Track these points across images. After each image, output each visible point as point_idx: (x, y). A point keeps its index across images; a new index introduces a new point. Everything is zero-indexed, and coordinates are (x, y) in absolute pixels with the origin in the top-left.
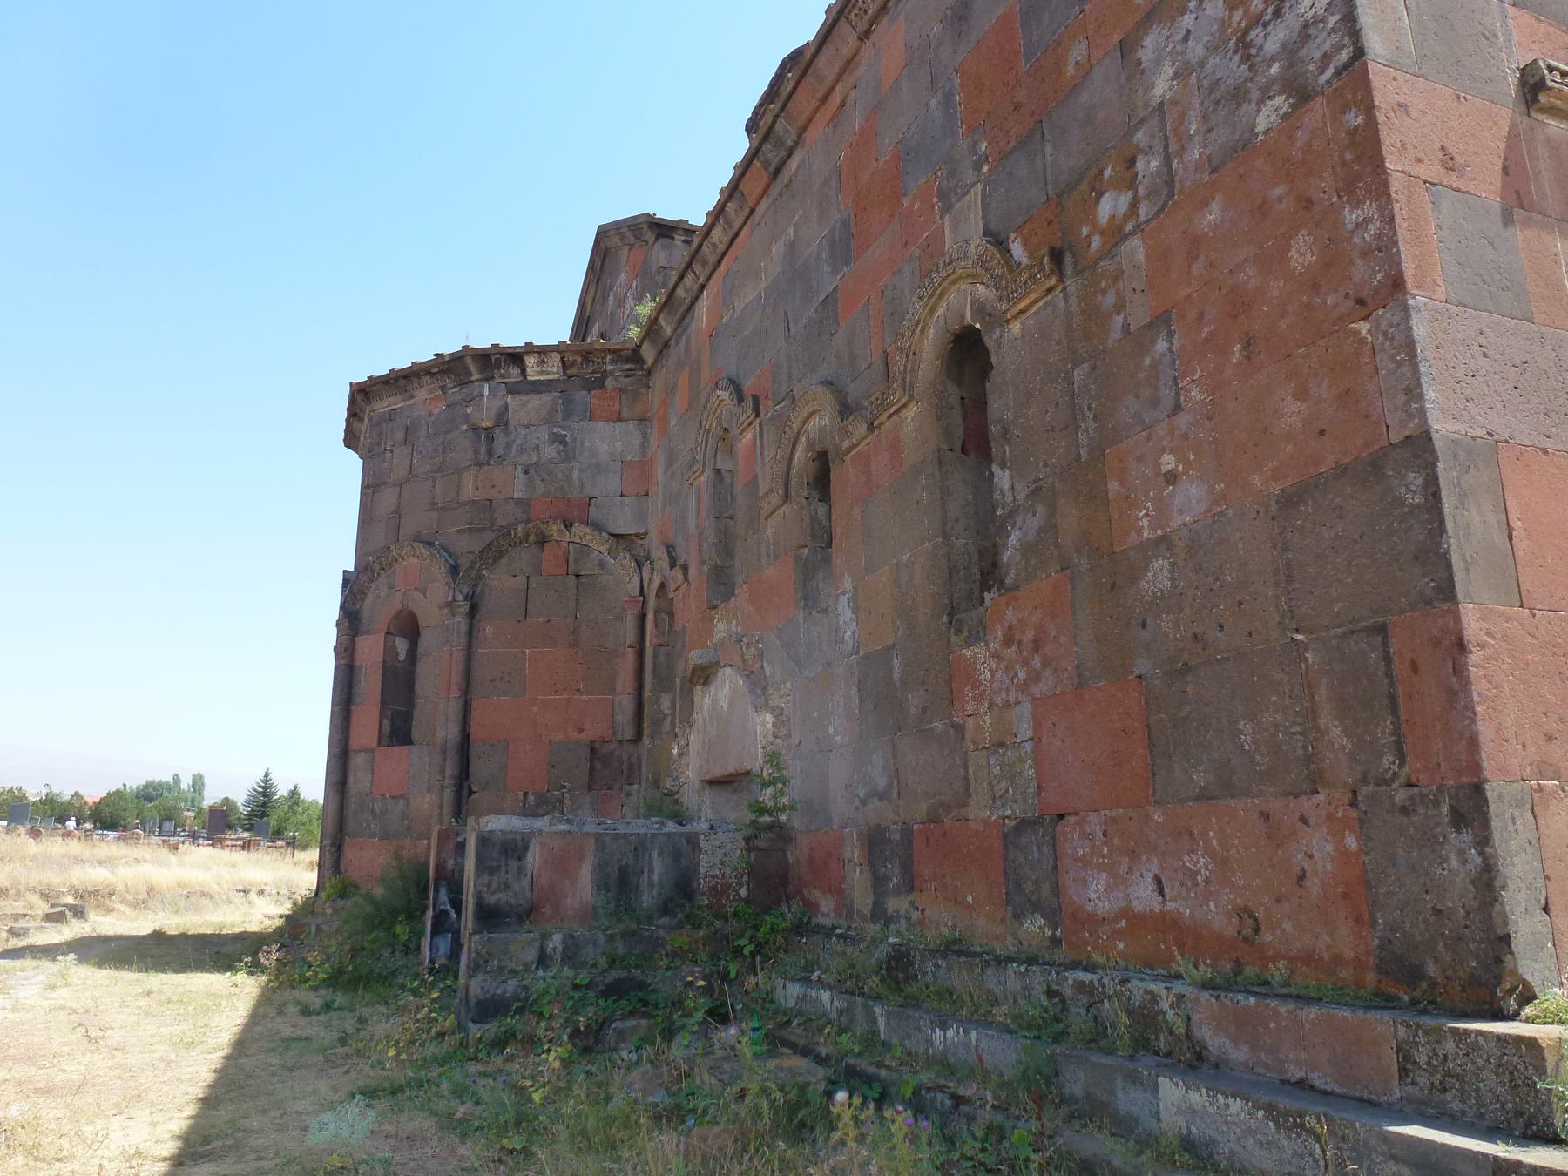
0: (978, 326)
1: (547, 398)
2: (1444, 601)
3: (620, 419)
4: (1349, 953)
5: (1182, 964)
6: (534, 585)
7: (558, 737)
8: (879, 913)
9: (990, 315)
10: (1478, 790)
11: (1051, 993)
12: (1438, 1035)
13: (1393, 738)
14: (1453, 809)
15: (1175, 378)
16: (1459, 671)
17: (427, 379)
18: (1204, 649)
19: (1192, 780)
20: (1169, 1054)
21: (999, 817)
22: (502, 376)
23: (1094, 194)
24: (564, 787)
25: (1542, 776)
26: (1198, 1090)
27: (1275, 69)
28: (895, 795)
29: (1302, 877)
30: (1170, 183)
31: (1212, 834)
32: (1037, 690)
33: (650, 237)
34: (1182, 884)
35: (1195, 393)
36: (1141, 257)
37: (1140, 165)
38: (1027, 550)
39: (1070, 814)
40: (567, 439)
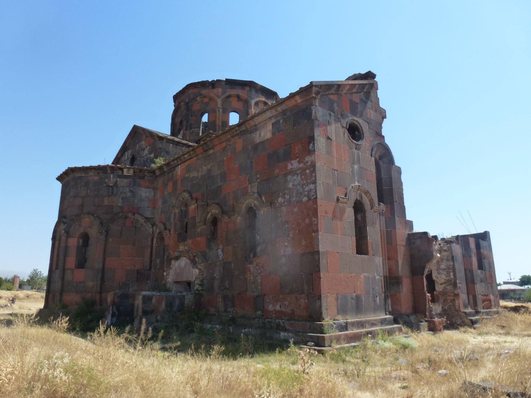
1: (129, 180)
3: (148, 188)
5: (283, 317)
7: (129, 268)
10: (320, 295)
11: (263, 323)
16: (320, 281)
17: (94, 170)
22: (117, 173)
27: (306, 193)
29: (300, 306)
30: (290, 201)
32: (262, 274)
35: (291, 235)
36: (285, 210)
37: (286, 196)
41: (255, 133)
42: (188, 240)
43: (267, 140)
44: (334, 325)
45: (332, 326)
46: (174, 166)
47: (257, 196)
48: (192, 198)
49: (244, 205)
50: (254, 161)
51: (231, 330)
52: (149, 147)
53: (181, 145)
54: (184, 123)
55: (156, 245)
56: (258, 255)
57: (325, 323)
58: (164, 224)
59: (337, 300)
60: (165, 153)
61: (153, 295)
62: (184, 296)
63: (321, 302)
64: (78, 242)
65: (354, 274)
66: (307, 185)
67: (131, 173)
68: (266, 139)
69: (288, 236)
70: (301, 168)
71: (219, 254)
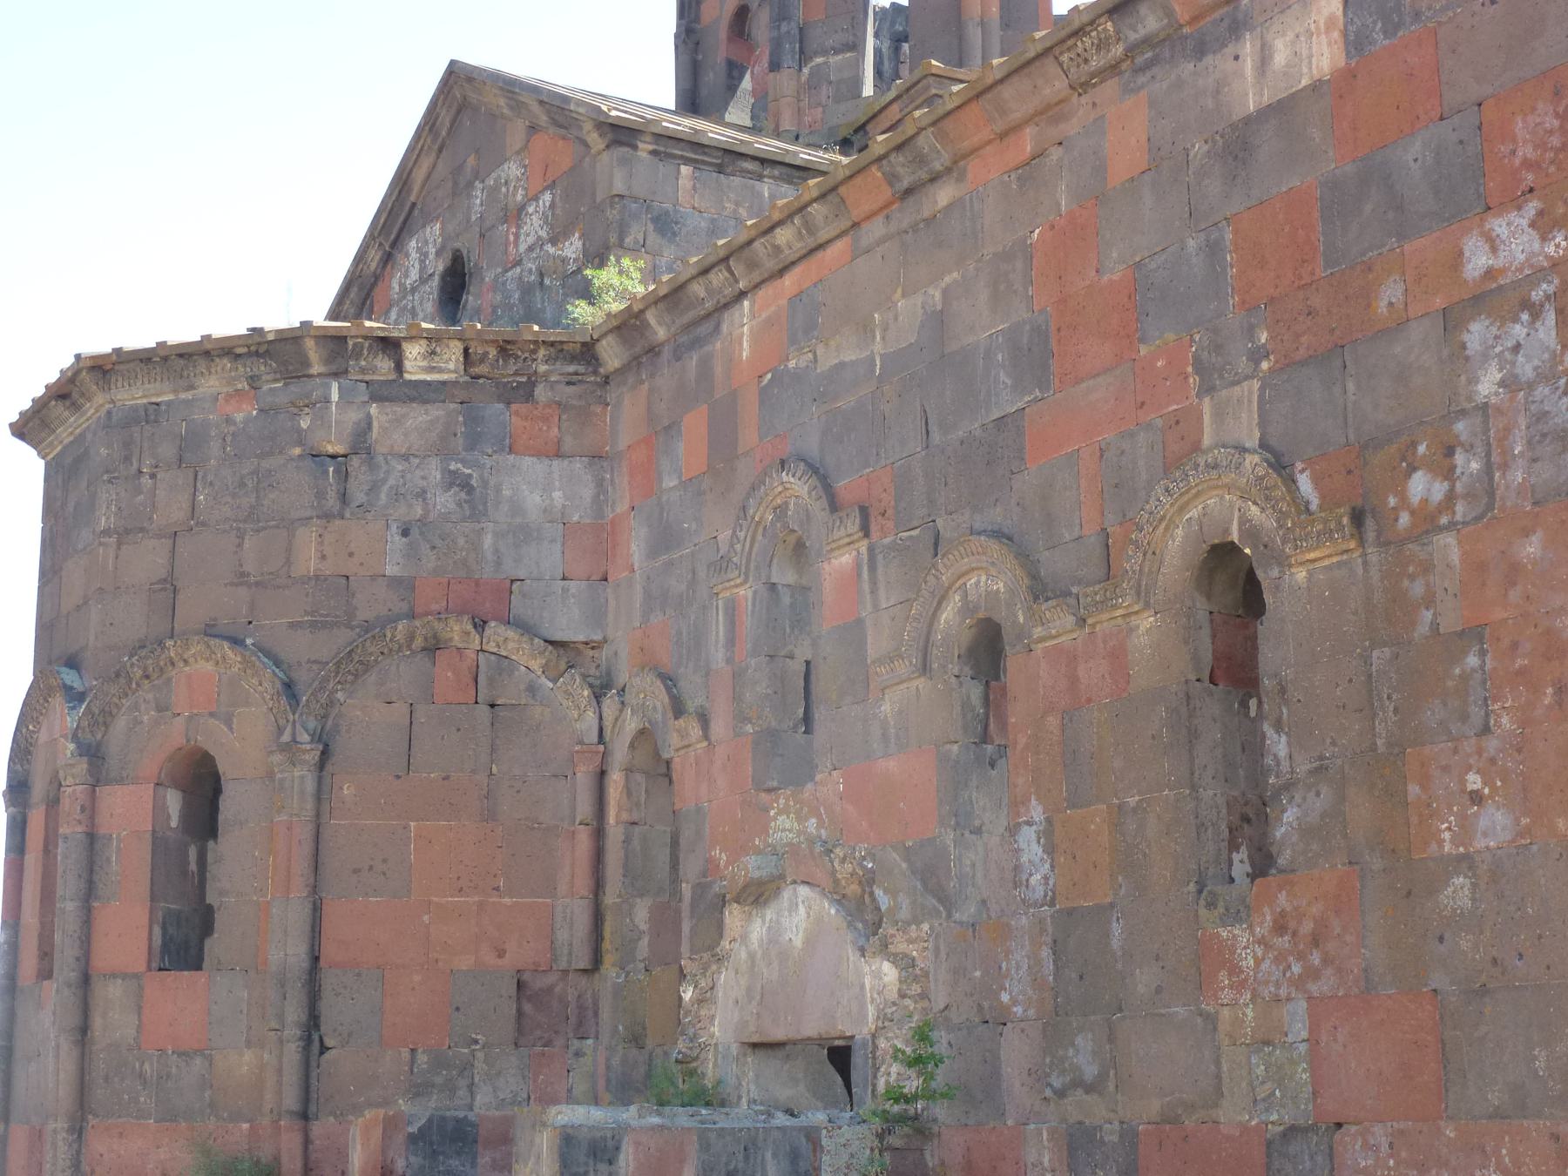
0: (1247, 551)
1: (436, 412)
3: (559, 455)
6: (420, 717)
7: (464, 963)
9: (1266, 546)
15: (1486, 699)
17: (227, 363)
18: (1503, 974)
19: (1487, 1100)
22: (363, 371)
23: (1404, 464)
24: (476, 1042)
28: (1111, 1087)
30: (1491, 493)
31: (1504, 1151)
32: (1314, 988)
33: (596, 141)
35: (1505, 720)
36: (1455, 556)
37: (1459, 458)
38: (1307, 831)
40: (474, 482)
41: (1230, 50)
42: (818, 777)
43: (1316, 86)
46: (709, 305)
47: (1261, 472)
48: (834, 506)
49: (1179, 532)
50: (1229, 236)
52: (547, 197)
53: (748, 165)
54: (761, 26)
55: (625, 816)
56: (1281, 861)
58: (668, 680)
60: (651, 227)
61: (621, 1130)
62: (812, 1135)
64: (159, 809)
67: (451, 366)
68: (1304, 82)
69: (1486, 730)
70: (1555, 264)
71: (1024, 859)
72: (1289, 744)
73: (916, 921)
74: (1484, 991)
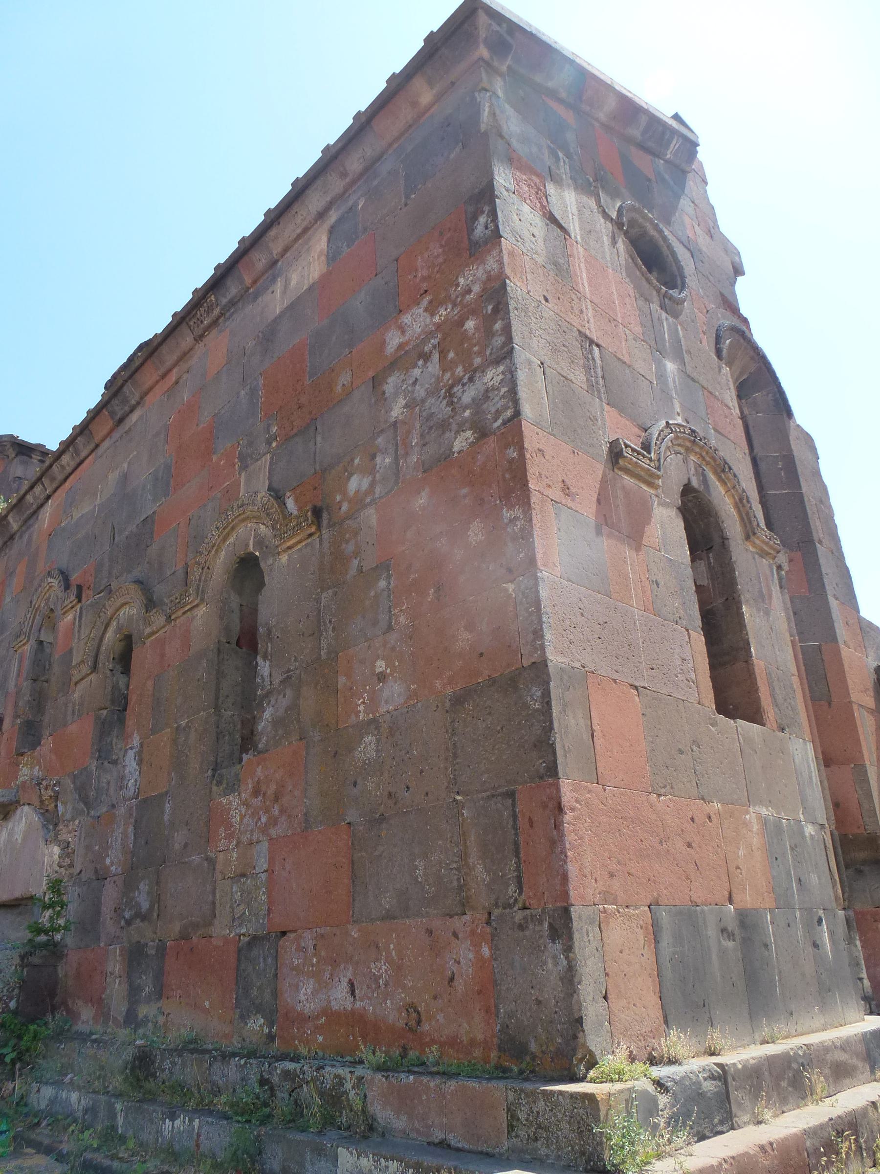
0: (257, 554)
2: (550, 776)
4: (480, 1037)
5: (364, 1052)
8: (131, 1019)
9: (267, 547)
10: (566, 911)
11: (263, 1082)
12: (533, 1096)
13: (515, 874)
14: (551, 925)
15: (390, 607)
16: (558, 826)
18: (395, 804)
19: (381, 905)
20: (348, 1128)
21: (236, 935)
23: (346, 474)
25: (606, 902)
26: (368, 1157)
27: (467, 413)
28: (155, 915)
29: (452, 979)
30: (397, 473)
31: (392, 946)
32: (273, 832)
34: (368, 987)
36: (374, 521)
37: (378, 460)
38: (277, 723)
39: (290, 931)
44: (663, 1100)
45: (651, 1108)
51: (120, 1120)
57: (606, 1088)
59: (657, 942)
63: (569, 948)
65: (717, 806)
66: (471, 379)
72: (271, 666)
73: (73, 819)
74: (383, 818)
